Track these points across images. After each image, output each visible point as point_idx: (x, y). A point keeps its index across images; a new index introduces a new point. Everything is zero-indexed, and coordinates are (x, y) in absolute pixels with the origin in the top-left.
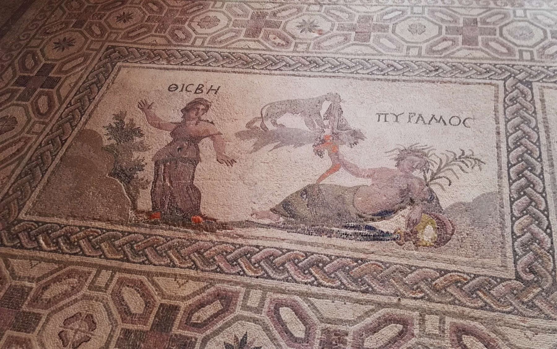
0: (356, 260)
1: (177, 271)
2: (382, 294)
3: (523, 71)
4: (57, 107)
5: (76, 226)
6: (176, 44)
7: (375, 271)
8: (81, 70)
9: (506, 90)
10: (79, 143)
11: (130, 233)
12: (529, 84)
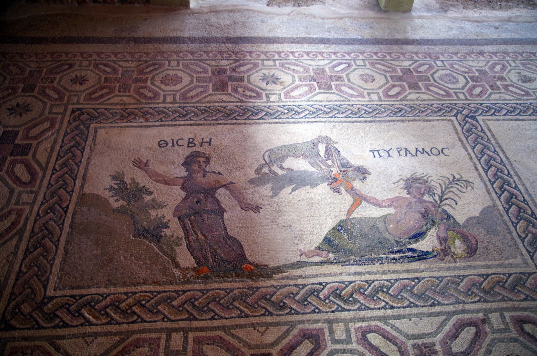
0: (413, 280)
1: (252, 320)
2: (447, 305)
3: (465, 108)
4: (40, 175)
5: (121, 293)
6: (147, 102)
7: (433, 286)
8: (52, 134)
9: (460, 124)
10: (84, 209)
11: (184, 292)
12: (474, 118)
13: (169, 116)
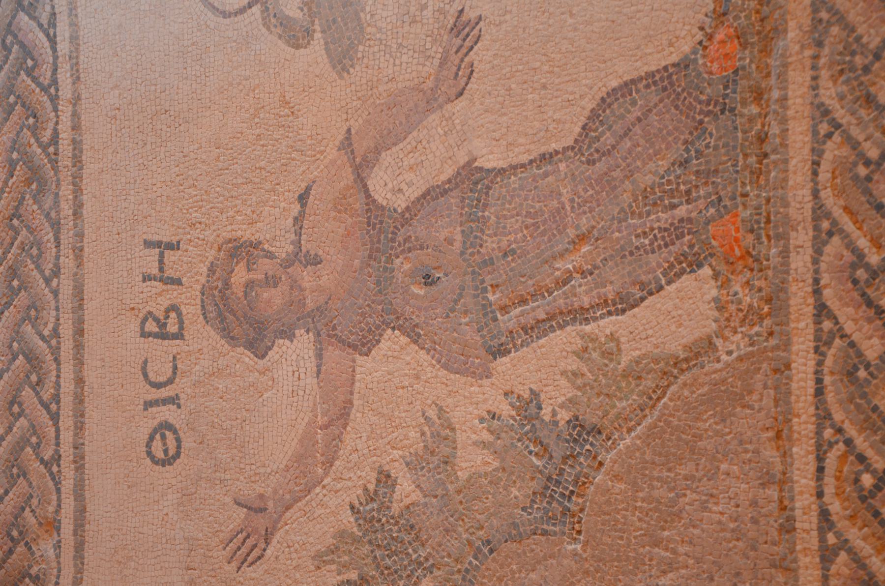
11: (822, 311)
13: (34, 429)
